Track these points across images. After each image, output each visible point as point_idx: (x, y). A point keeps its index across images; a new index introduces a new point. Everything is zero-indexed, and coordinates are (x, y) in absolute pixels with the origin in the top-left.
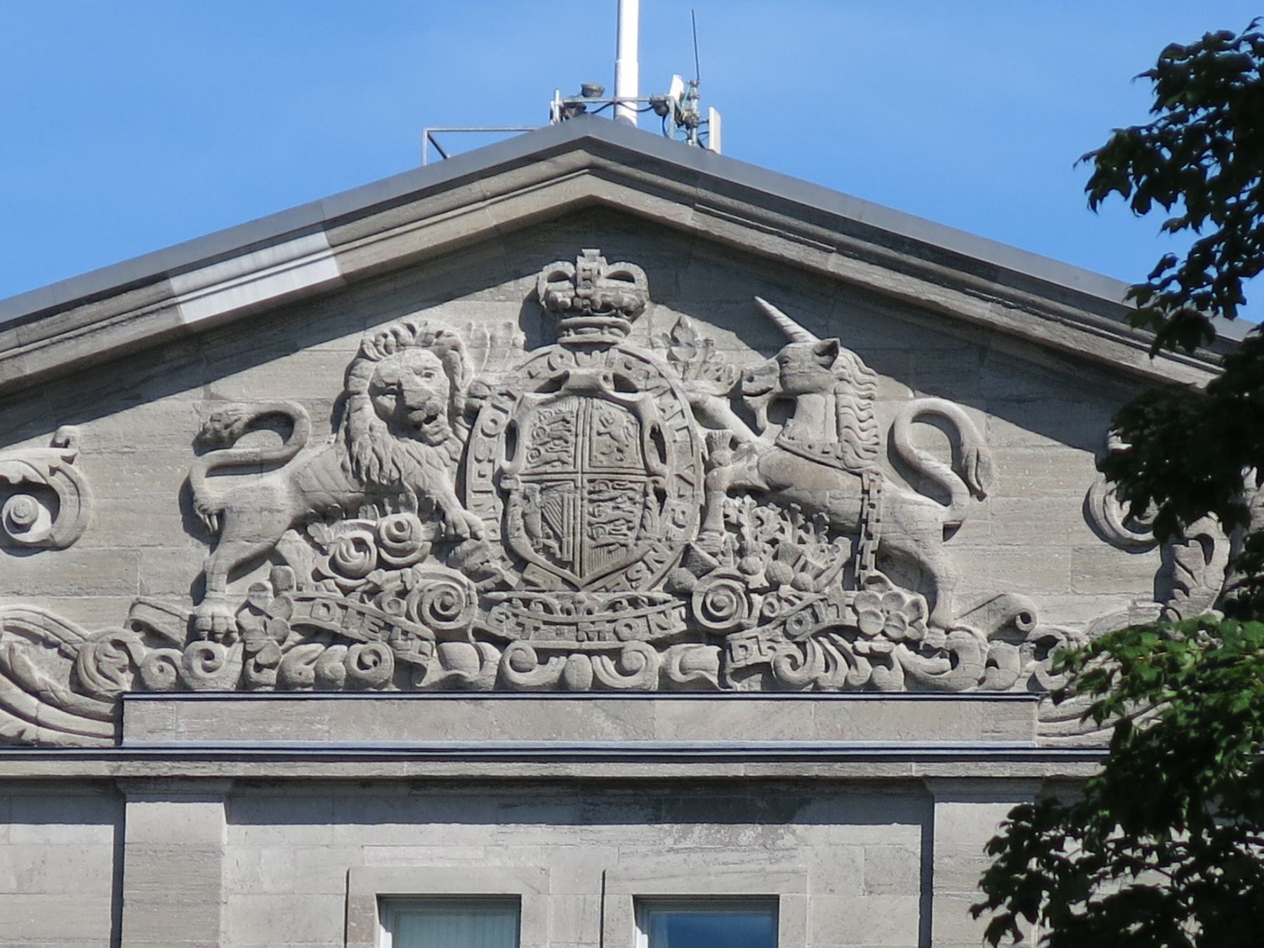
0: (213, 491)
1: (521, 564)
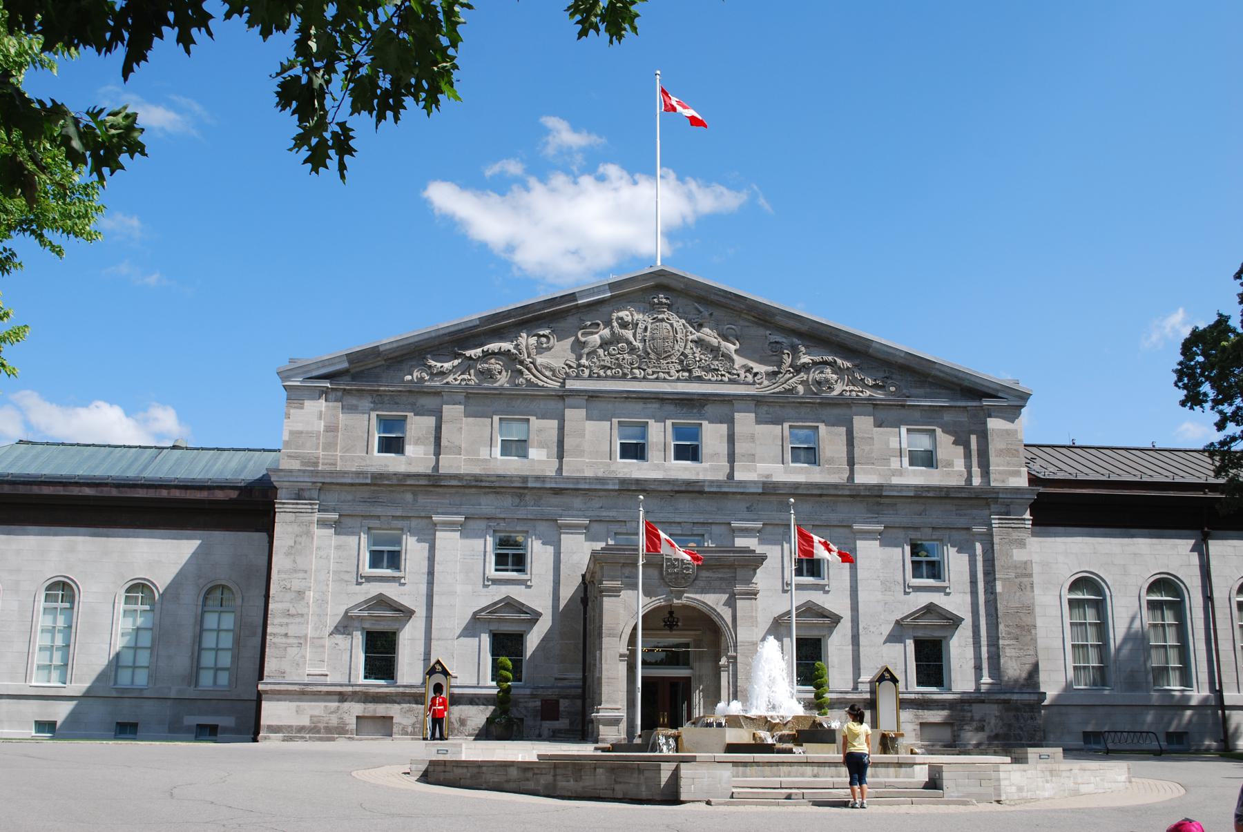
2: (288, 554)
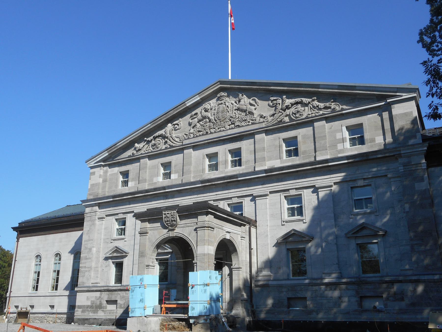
1: (216, 120)
2: (87, 234)
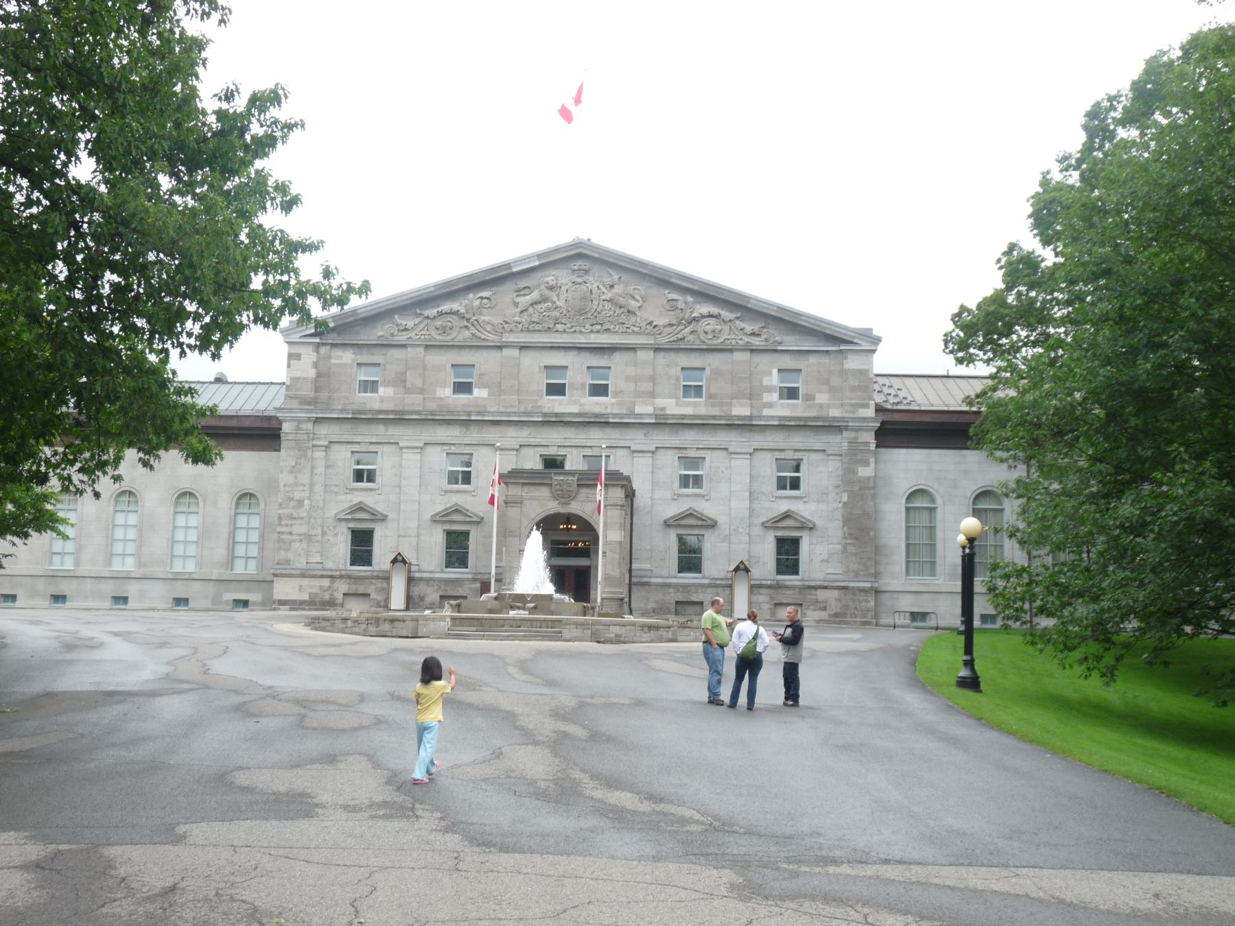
0: (519, 300)
2: (291, 472)
